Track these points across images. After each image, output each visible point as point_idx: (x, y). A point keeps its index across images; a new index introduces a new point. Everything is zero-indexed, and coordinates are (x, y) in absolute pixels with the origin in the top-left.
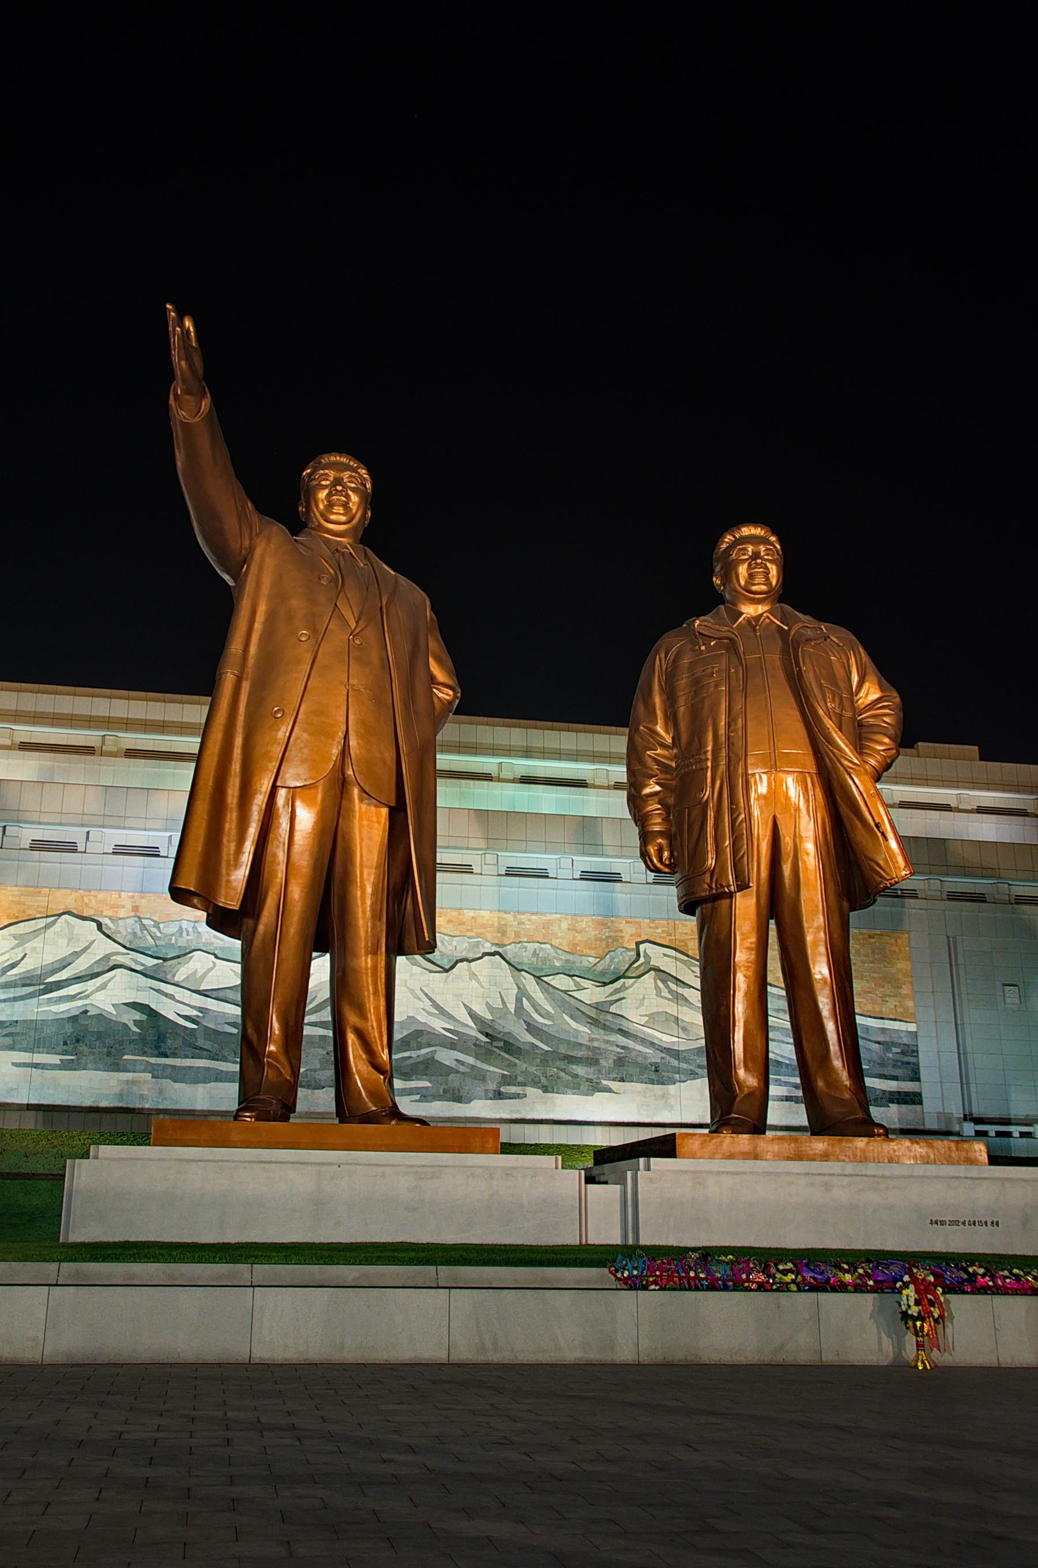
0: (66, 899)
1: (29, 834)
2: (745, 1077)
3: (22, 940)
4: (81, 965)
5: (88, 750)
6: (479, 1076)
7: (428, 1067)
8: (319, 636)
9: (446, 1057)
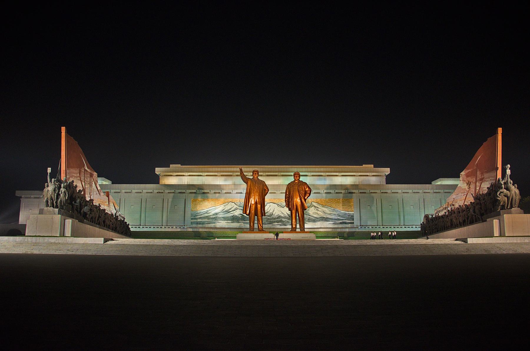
0: (231, 200)
1: (225, 191)
2: (294, 226)
3: (225, 206)
4: (233, 209)
5: (231, 176)
6: (289, 222)
7: (281, 221)
8: (254, 190)
9: (284, 220)
